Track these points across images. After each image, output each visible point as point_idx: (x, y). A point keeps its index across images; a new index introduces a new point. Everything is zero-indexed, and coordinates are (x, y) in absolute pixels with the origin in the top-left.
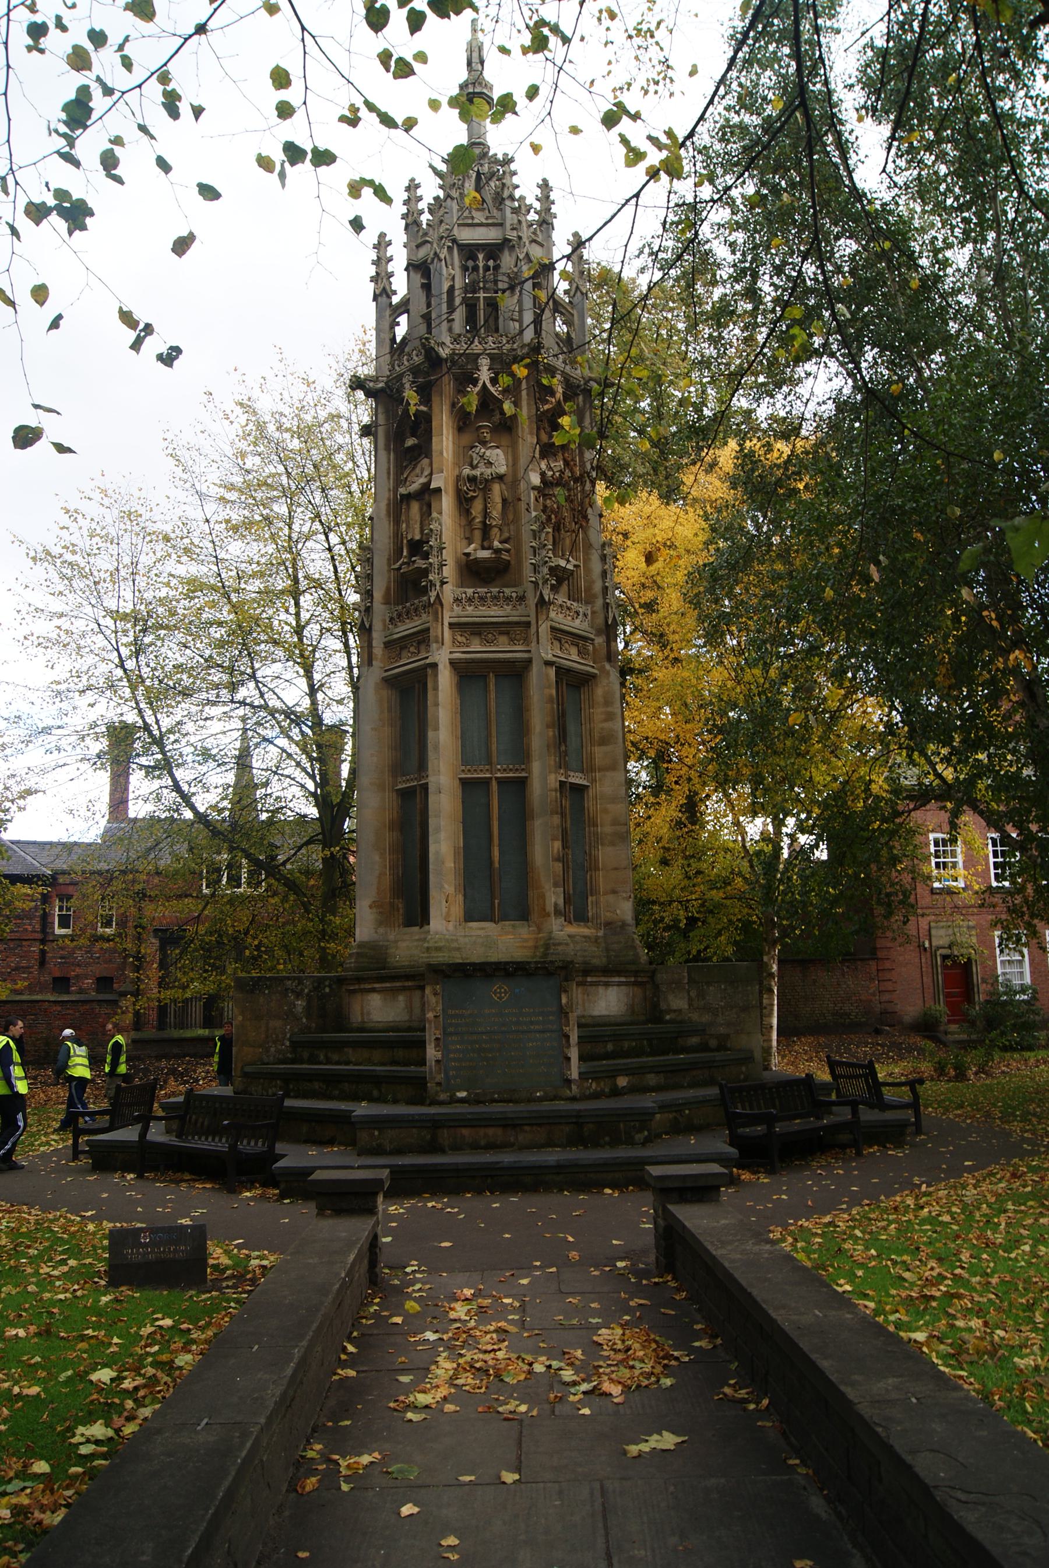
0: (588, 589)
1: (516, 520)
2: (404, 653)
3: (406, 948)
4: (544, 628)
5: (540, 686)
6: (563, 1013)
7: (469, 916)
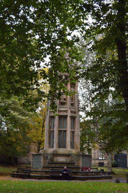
2: (61, 112)
3: (61, 151)
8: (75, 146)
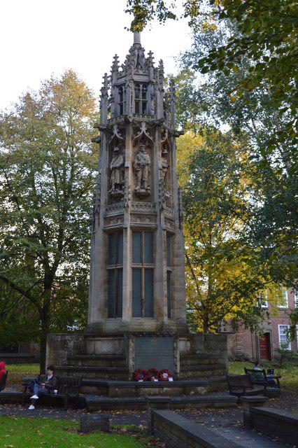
0: (173, 204)
1: (153, 179)
2: (112, 222)
3: (111, 325)
4: (162, 217)
5: (160, 237)
6: (175, 349)
7: (134, 315)
8: (155, 309)
